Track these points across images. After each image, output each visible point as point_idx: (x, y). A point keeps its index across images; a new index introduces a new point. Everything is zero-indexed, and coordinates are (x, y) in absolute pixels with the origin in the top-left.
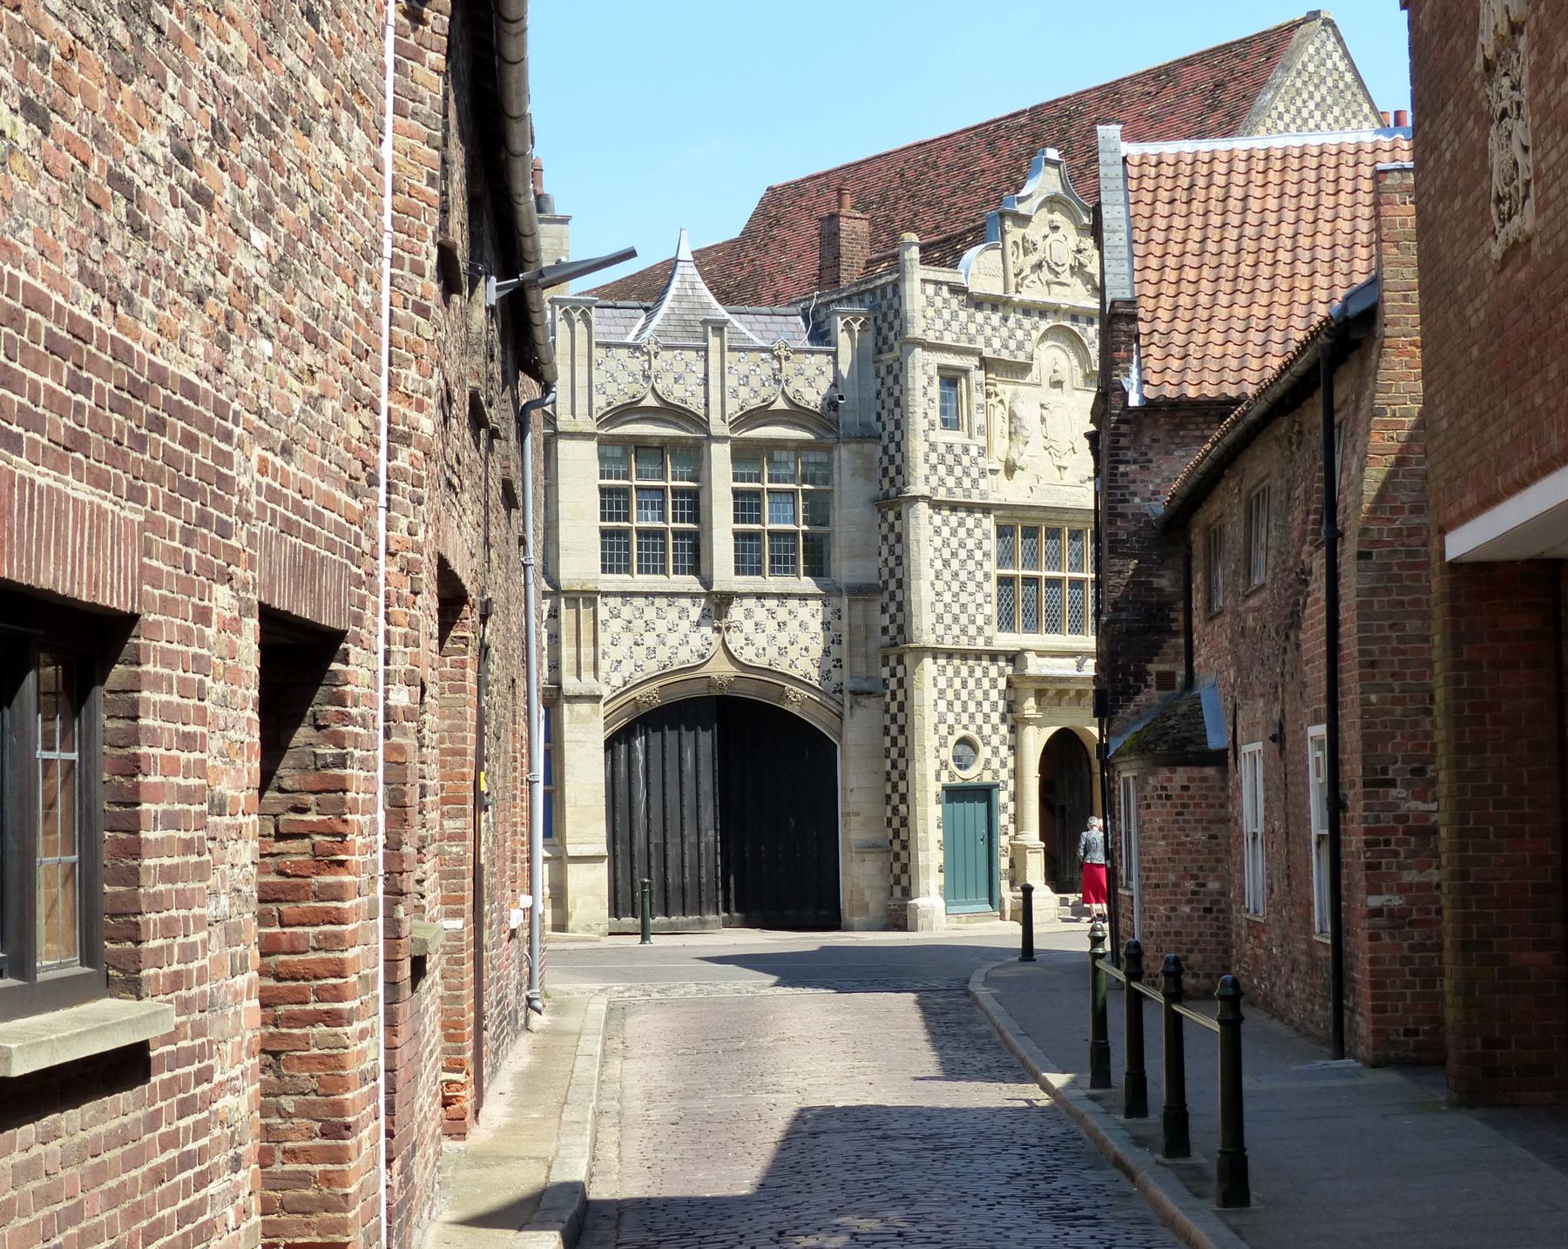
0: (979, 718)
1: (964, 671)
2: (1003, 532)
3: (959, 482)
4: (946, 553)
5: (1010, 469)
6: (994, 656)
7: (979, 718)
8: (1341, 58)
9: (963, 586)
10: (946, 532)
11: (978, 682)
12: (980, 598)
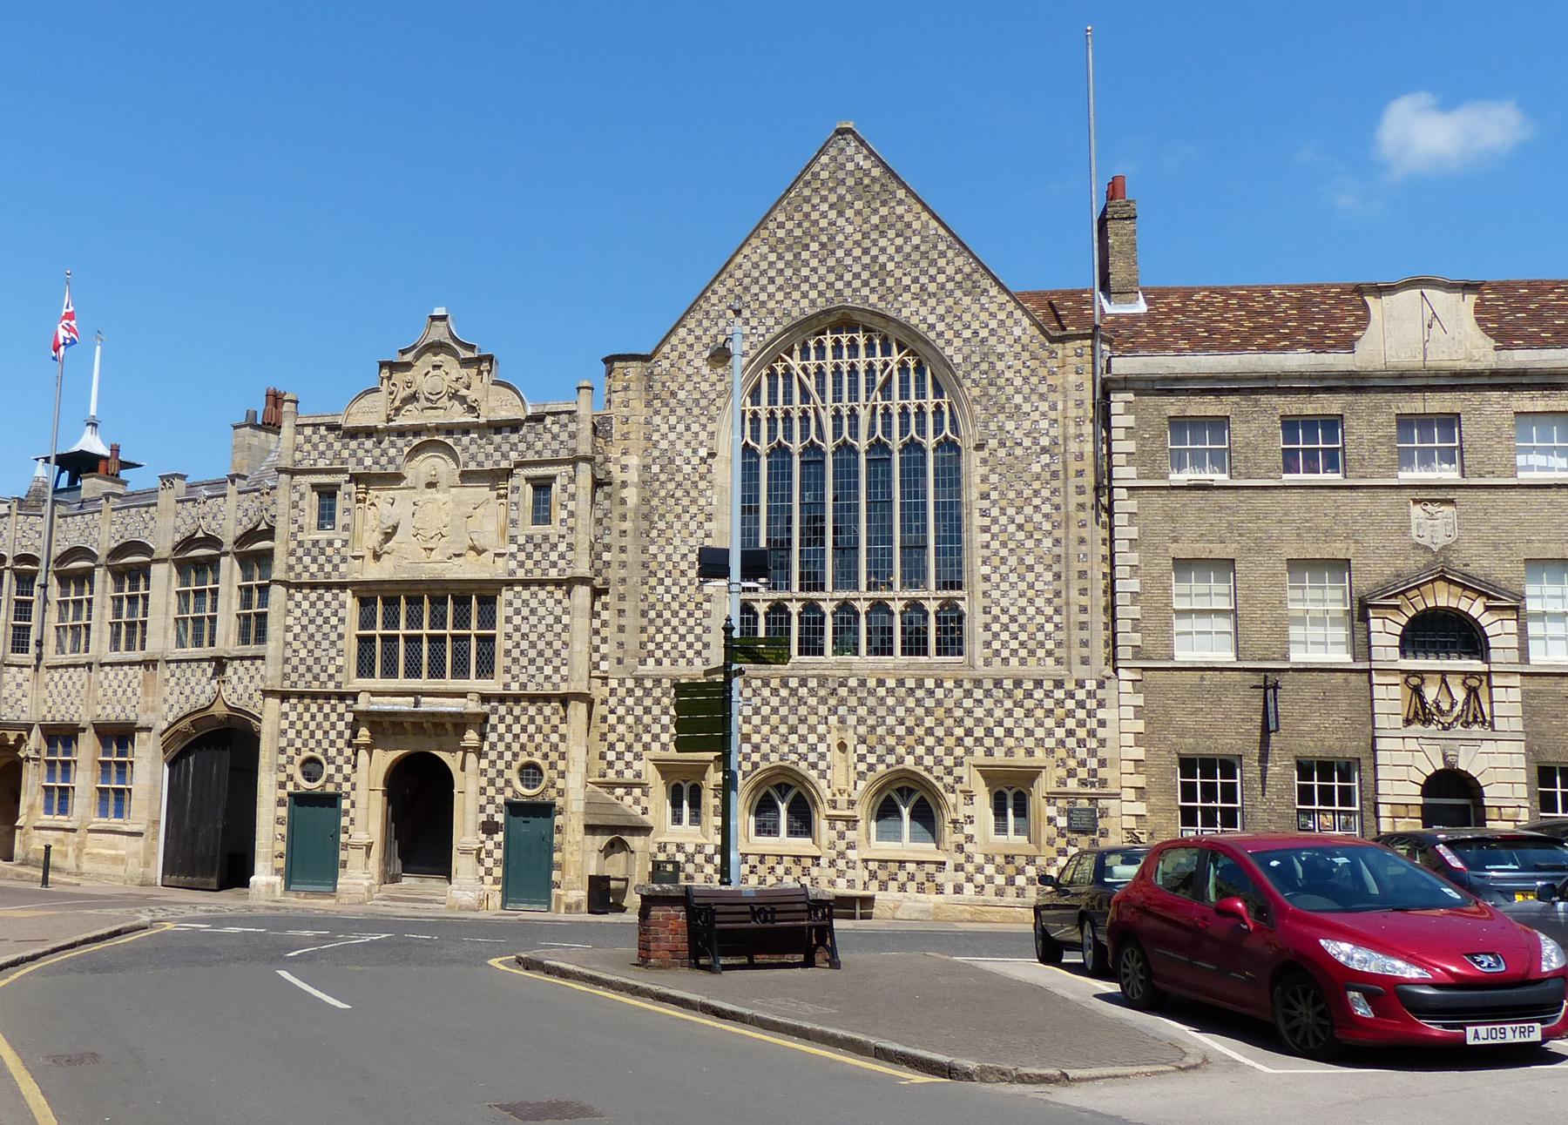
0: (325, 744)
1: (314, 708)
2: (366, 603)
3: (321, 568)
4: (305, 621)
5: (377, 557)
6: (342, 697)
7: (325, 744)
8: (866, 158)
9: (318, 644)
10: (306, 605)
11: (326, 716)
12: (333, 653)
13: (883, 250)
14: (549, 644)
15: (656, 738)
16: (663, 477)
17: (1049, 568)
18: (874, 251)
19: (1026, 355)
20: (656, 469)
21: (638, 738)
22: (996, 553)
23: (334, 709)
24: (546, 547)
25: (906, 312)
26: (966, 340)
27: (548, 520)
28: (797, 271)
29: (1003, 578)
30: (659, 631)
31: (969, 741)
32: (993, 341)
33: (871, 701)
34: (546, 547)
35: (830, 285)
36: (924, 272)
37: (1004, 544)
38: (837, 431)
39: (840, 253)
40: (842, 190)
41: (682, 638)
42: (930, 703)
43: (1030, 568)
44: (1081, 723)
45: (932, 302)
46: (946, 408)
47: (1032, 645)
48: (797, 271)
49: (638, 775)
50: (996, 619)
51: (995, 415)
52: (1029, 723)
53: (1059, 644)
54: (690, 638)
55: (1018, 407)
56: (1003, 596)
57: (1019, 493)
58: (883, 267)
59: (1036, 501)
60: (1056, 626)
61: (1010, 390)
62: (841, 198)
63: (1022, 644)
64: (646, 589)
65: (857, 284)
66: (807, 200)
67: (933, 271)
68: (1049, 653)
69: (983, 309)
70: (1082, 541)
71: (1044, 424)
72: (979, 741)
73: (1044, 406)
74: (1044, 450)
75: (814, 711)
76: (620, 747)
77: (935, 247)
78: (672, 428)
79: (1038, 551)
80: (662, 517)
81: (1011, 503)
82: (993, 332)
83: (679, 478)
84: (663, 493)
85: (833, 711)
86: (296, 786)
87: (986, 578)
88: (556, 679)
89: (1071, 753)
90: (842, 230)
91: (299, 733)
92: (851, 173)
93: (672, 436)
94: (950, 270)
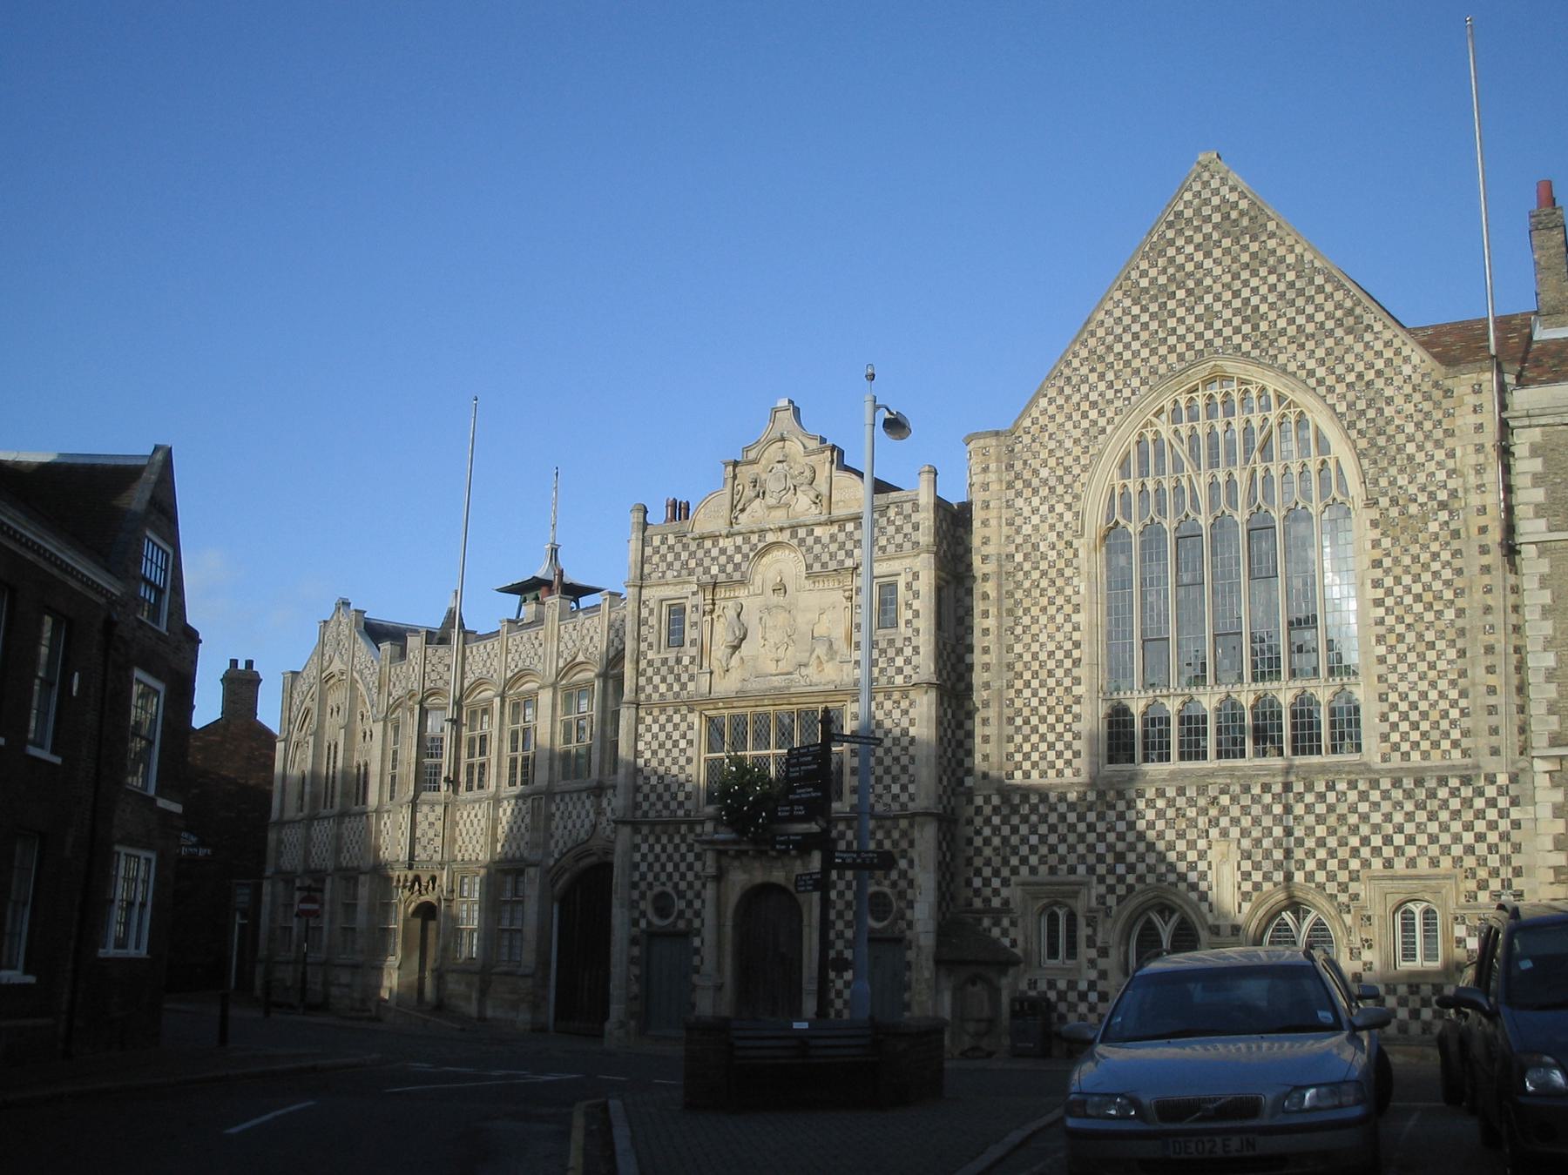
0: (676, 877)
4: (655, 745)
7: (676, 877)
11: (677, 848)
13: (1255, 291)
14: (896, 759)
15: (1024, 860)
16: (1027, 566)
17: (1452, 643)
18: (1246, 293)
19: (1417, 397)
20: (1019, 557)
21: (1006, 862)
22: (1391, 630)
23: (683, 839)
24: (891, 652)
25: (1282, 359)
26: (1350, 386)
27: (895, 625)
28: (1163, 323)
29: (1401, 658)
30: (1026, 739)
31: (1365, 852)
32: (1380, 383)
33: (1256, 810)
34: (891, 652)
35: (1199, 336)
36: (1301, 311)
37: (1400, 620)
38: (1213, 503)
39: (1208, 299)
40: (1207, 228)
41: (1051, 746)
42: (1320, 809)
43: (1431, 645)
44: (1493, 826)
45: (1310, 345)
46: (1332, 465)
47: (1435, 735)
48: (1163, 323)
49: (1006, 902)
50: (1394, 707)
51: (1384, 470)
52: (1433, 827)
53: (1466, 733)
54: (1060, 746)
55: (1411, 458)
56: (1401, 680)
57: (1415, 559)
58: (1256, 308)
59: (1436, 566)
60: (1462, 711)
61: (1400, 439)
62: (1207, 237)
63: (1424, 735)
64: (1012, 694)
65: (1228, 331)
66: (1171, 243)
67: (1310, 309)
68: (1455, 744)
69: (1367, 346)
70: (1488, 610)
71: (1441, 475)
72: (1377, 851)
73: (1440, 455)
74: (1443, 505)
75: (1193, 823)
76: (987, 872)
77: (1311, 281)
78: (1035, 511)
79: (1440, 625)
80: (1027, 611)
81: (1407, 570)
82: (1379, 373)
83: (1044, 565)
84: (1027, 584)
85: (1214, 822)
86: (649, 923)
87: (1382, 660)
88: (904, 798)
89: (1482, 861)
90: (1210, 272)
91: (650, 866)
92: (1217, 209)
93: (1036, 520)
94: (1329, 306)
